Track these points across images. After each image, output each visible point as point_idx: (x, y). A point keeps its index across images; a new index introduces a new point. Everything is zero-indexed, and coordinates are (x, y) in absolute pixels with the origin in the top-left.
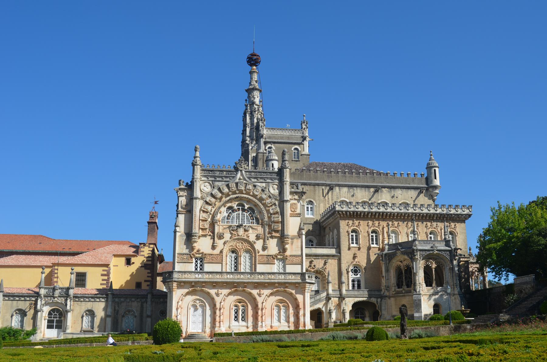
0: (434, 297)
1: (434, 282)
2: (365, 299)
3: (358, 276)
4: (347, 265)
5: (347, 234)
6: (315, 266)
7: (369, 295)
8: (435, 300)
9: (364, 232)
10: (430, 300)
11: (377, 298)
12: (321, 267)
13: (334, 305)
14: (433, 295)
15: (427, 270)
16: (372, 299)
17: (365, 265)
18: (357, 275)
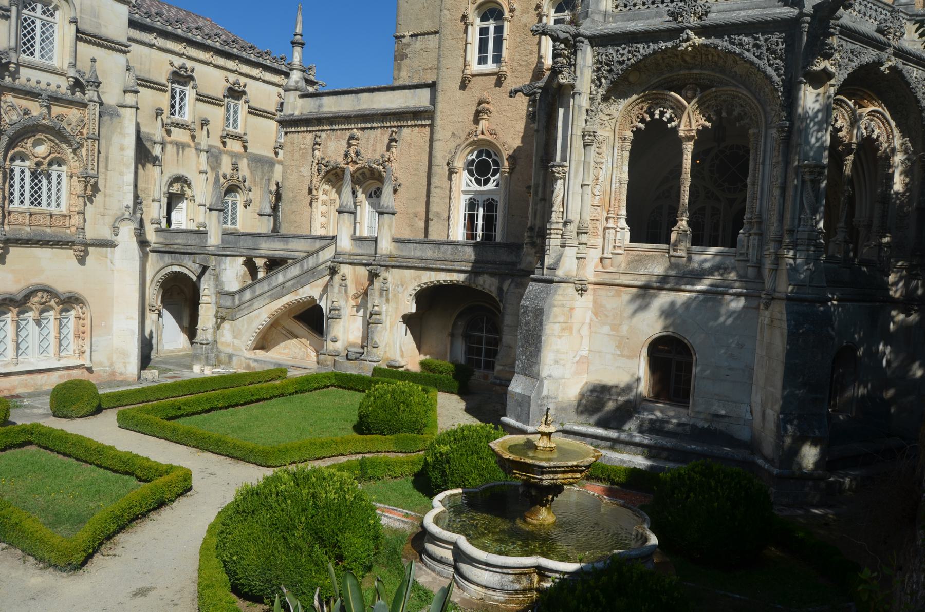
0: (664, 298)
1: (683, 224)
2: (459, 278)
3: (491, 186)
4: (452, 145)
5: (461, 26)
6: (357, 154)
7: (476, 262)
8: (669, 312)
9: (525, 11)
10: (643, 308)
11: (502, 277)
12: (378, 157)
13: (352, 291)
14: (663, 283)
15: (651, 150)
16: (480, 280)
17: (517, 143)
18: (486, 182)
